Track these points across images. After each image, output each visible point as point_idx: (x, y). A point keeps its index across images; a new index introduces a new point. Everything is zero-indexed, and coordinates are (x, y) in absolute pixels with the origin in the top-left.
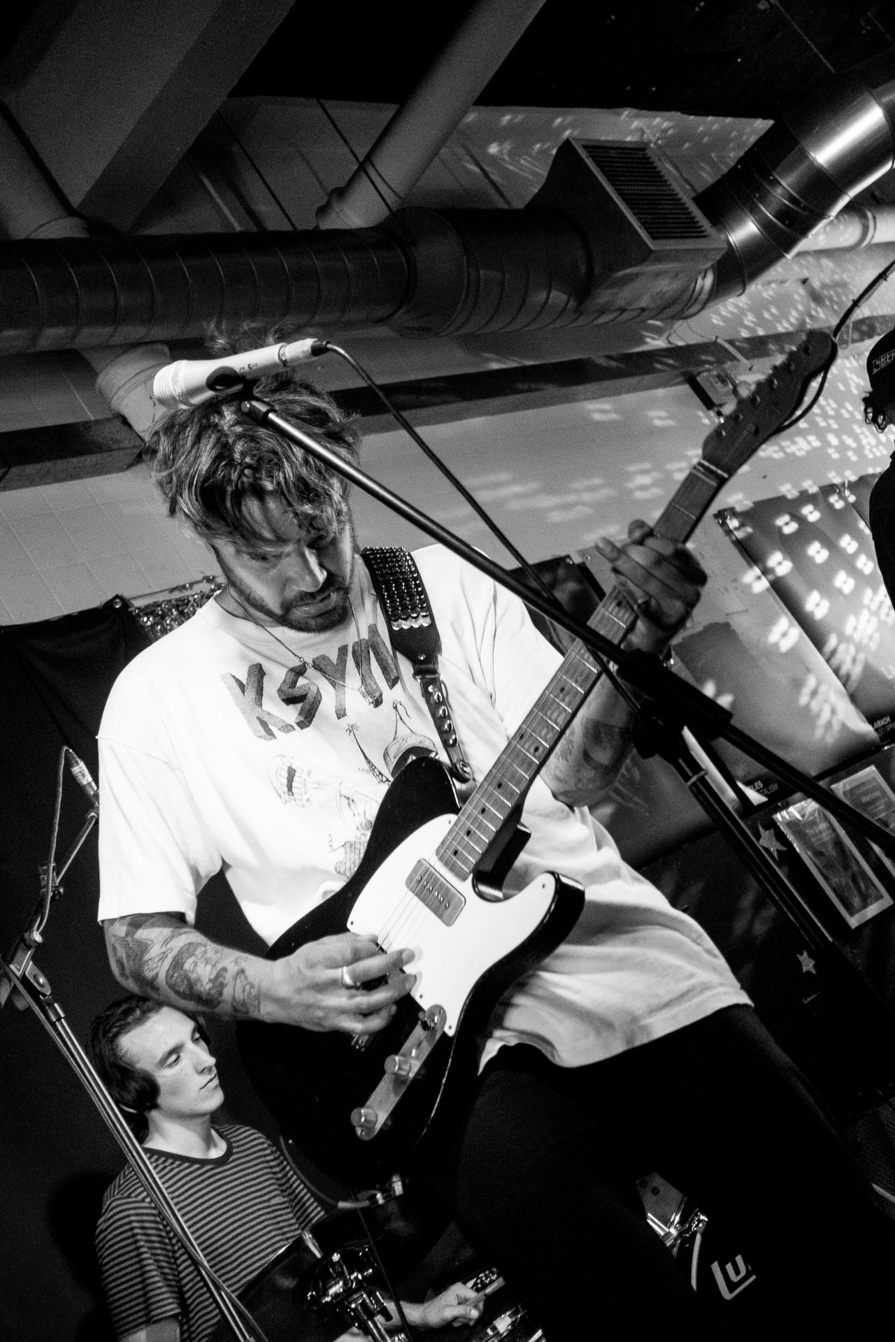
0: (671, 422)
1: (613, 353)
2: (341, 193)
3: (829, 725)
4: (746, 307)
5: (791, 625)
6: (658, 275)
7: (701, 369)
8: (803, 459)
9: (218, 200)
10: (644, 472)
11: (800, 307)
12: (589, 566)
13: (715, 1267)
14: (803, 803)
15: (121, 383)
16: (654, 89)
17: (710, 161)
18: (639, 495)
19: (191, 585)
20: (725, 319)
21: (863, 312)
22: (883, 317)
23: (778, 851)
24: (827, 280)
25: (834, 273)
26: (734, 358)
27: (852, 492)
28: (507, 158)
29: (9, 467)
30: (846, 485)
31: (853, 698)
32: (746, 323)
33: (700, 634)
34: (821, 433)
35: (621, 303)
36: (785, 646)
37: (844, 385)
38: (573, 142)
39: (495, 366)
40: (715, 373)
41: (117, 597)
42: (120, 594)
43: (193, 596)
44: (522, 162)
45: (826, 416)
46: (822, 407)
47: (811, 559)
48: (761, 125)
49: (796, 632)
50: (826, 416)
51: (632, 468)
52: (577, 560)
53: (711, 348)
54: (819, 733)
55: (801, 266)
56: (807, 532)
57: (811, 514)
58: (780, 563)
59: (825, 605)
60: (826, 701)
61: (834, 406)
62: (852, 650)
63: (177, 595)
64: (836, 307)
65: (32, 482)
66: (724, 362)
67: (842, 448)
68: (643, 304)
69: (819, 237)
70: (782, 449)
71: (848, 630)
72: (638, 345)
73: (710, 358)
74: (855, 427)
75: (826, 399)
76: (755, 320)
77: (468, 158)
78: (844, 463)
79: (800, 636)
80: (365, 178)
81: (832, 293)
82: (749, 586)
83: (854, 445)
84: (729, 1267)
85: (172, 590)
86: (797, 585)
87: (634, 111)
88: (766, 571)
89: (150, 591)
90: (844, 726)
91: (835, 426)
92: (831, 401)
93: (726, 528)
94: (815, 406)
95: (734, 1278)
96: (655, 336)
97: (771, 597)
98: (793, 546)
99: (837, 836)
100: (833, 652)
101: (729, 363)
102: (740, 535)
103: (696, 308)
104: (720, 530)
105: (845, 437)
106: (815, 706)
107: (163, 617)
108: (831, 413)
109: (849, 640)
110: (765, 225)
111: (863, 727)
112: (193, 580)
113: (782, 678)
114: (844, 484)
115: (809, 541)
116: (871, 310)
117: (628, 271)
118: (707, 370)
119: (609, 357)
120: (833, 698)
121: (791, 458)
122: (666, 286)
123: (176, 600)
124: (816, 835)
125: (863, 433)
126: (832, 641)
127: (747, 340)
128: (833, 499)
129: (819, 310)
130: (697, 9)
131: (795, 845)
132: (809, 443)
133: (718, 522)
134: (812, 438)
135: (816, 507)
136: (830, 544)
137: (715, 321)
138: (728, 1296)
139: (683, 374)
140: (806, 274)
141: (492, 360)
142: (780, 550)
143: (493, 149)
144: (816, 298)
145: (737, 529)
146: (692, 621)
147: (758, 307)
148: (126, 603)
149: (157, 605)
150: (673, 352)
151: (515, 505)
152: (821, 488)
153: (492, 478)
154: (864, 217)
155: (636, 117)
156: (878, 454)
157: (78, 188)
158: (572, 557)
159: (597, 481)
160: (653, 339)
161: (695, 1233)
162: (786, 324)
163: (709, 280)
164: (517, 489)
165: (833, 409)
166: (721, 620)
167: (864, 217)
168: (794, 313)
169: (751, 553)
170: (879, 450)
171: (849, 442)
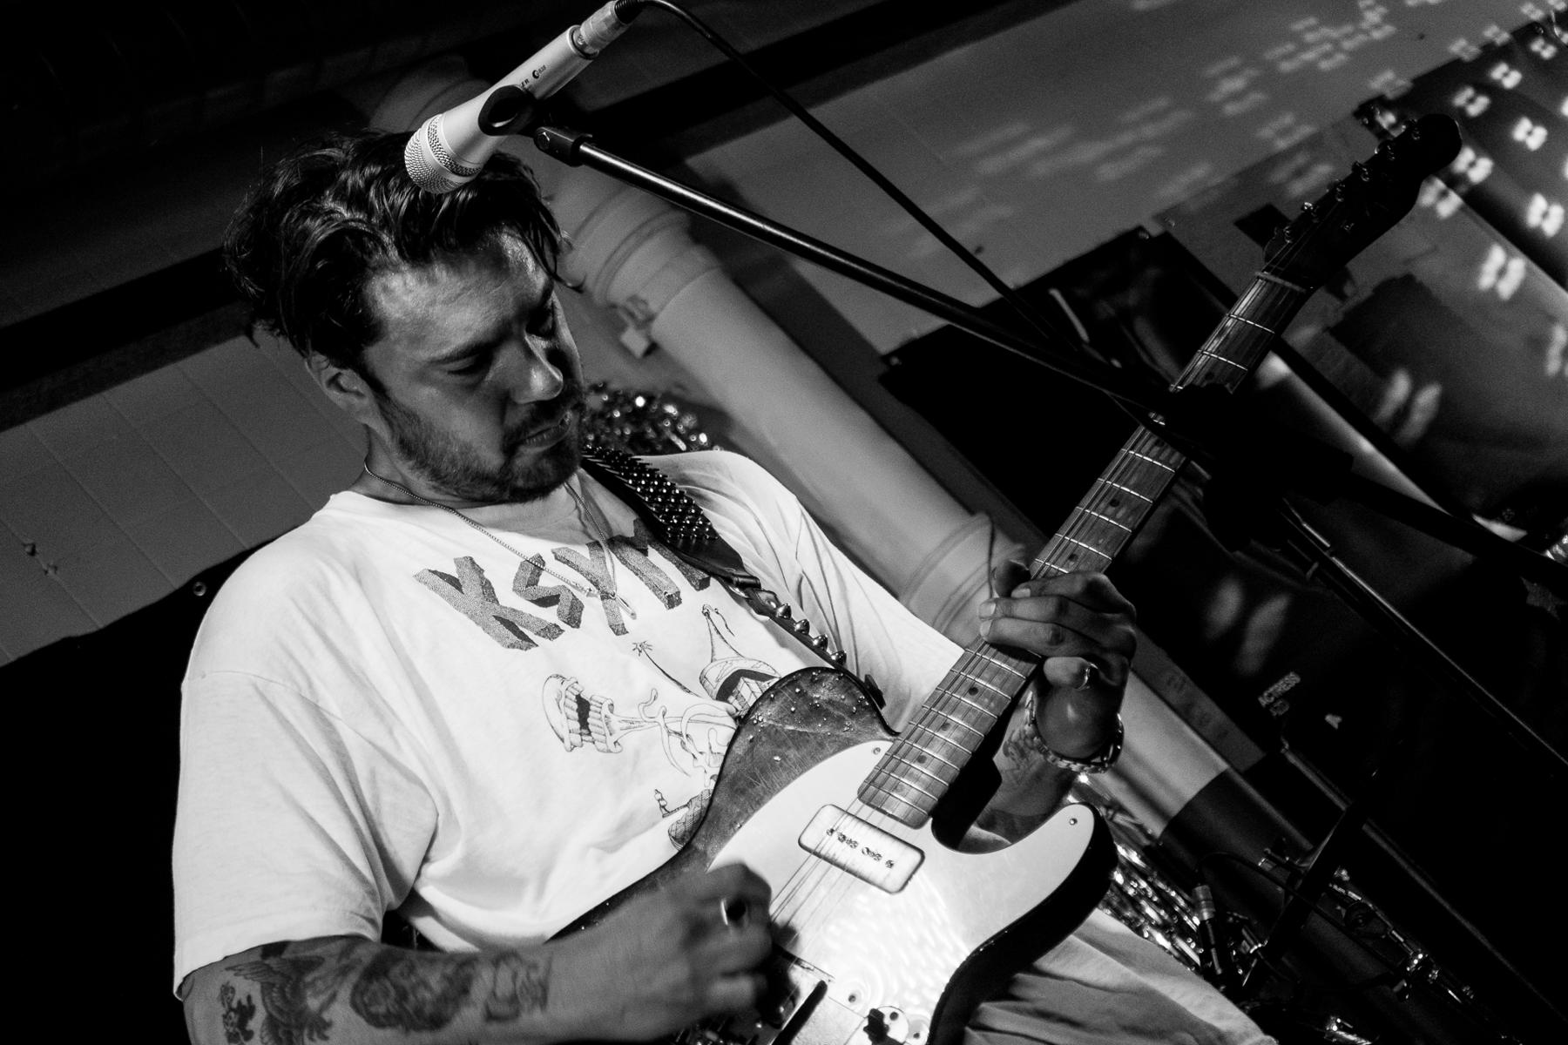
5: (1509, 255)
10: (1231, 73)
12: (1175, 235)
18: (1231, 109)
33: (1369, 300)
36: (1507, 288)
47: (1521, 146)
49: (1518, 266)
51: (1214, 70)
52: (1155, 230)
56: (1506, 106)
57: (1508, 77)
58: (1472, 165)
79: (1528, 269)
82: (1432, 210)
86: (1506, 191)
88: (1454, 182)
97: (1468, 220)
114: (1548, 19)
115: (1512, 120)
128: (1537, 46)
133: (1364, 124)
135: (1513, 65)
145: (1394, 126)
146: (1353, 283)
151: (1041, 169)
152: (1514, 33)
153: (997, 136)
158: (1145, 225)
159: (1162, 102)
164: (1039, 143)
166: (1397, 272)
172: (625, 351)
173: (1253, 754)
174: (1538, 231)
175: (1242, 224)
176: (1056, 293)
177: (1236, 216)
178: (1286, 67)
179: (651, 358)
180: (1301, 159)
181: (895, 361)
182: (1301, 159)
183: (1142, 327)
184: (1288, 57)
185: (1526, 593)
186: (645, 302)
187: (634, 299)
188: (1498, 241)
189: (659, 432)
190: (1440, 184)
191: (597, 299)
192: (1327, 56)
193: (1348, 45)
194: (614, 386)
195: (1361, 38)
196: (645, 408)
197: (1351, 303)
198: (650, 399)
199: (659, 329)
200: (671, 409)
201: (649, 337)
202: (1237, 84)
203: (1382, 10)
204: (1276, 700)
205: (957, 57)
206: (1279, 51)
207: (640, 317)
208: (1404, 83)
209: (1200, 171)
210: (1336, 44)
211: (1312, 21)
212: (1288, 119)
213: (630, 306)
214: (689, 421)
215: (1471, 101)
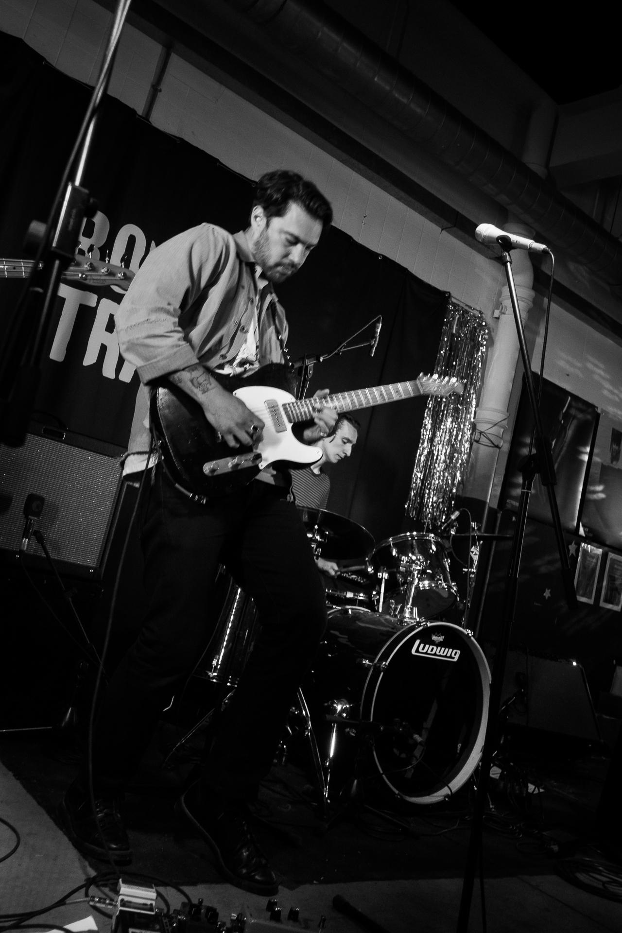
13: (418, 642)
19: (474, 309)
29: (455, 226)
33: (616, 469)
41: (449, 292)
52: (599, 411)
63: (467, 308)
65: (457, 237)
84: (422, 645)
85: (467, 305)
89: (460, 299)
95: (420, 650)
107: (457, 311)
112: (476, 308)
138: (413, 652)
148: (450, 296)
149: (458, 305)
151: (596, 377)
153: (597, 362)
161: (421, 626)
164: (602, 373)
173: (495, 506)
175: (613, 430)
176: (570, 398)
179: (495, 319)
183: (575, 422)
186: (507, 310)
187: (506, 307)
189: (480, 332)
191: (500, 299)
194: (483, 315)
196: (483, 326)
197: (612, 465)
199: (503, 317)
200: (486, 331)
205: (610, 342)
213: (504, 307)
214: (487, 337)
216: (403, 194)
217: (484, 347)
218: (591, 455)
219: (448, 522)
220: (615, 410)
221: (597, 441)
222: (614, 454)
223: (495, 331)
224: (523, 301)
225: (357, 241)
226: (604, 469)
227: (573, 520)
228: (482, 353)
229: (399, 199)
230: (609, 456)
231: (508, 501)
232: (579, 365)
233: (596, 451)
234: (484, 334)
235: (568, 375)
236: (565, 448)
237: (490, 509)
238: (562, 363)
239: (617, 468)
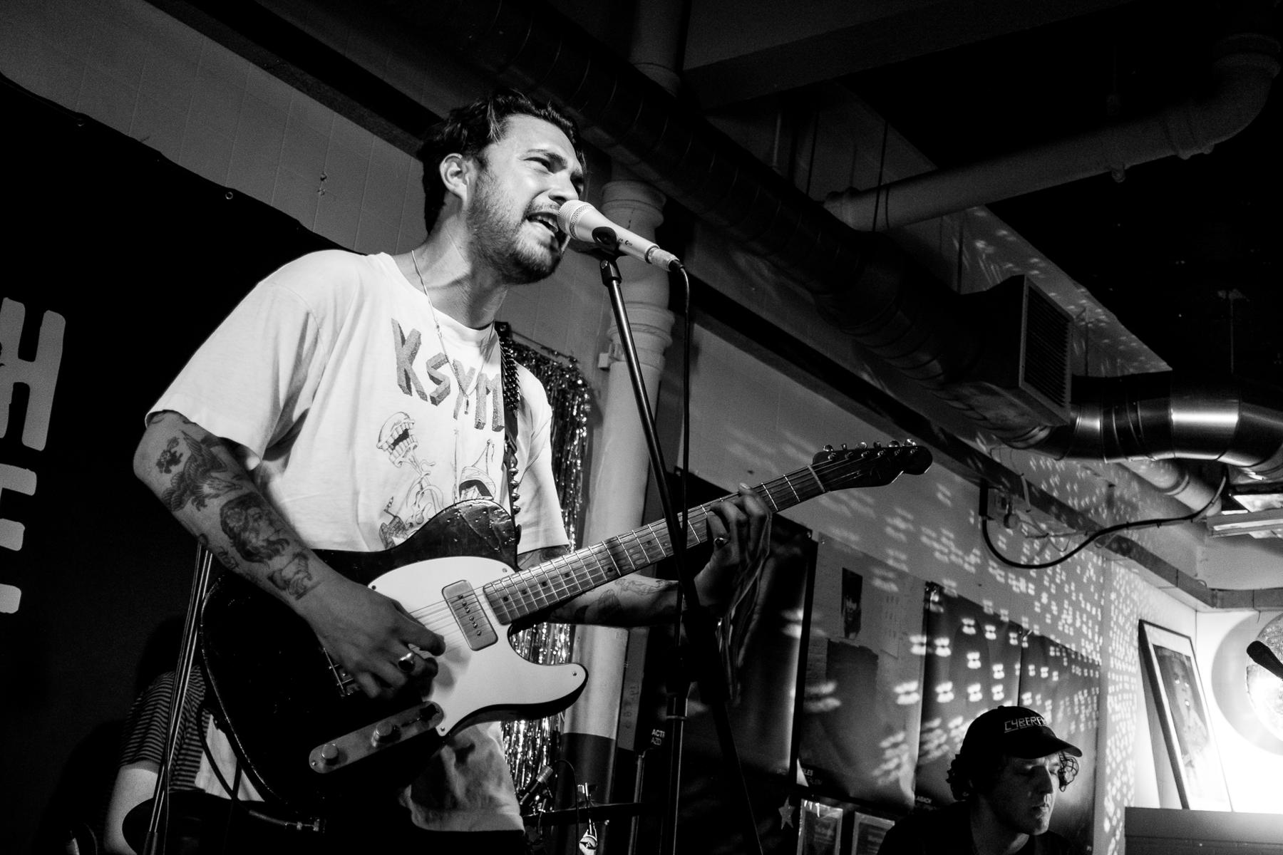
0: (948, 502)
1: (948, 430)
2: (854, 193)
3: (888, 773)
4: (1059, 470)
5: (917, 691)
6: (1012, 405)
7: (995, 486)
8: (1014, 593)
9: (777, 139)
10: (904, 519)
11: (1094, 499)
14: (829, 808)
15: (620, 198)
16: (1111, 289)
17: (1114, 365)
18: (889, 531)
19: (559, 354)
20: (1038, 466)
21: (1125, 533)
22: (1142, 548)
23: (786, 823)
24: (1126, 497)
25: (1135, 496)
26: (1023, 496)
27: (1028, 641)
28: (984, 256)
30: (1029, 633)
31: (918, 769)
32: (1051, 481)
33: (854, 647)
34: (1040, 588)
35: (973, 402)
36: (903, 700)
37: (1081, 571)
38: (1025, 279)
39: (866, 377)
40: (1003, 495)
41: (506, 324)
42: (509, 323)
43: (554, 362)
44: (992, 267)
45: (1052, 580)
46: (1054, 572)
47: (966, 661)
48: (1164, 366)
50: (1052, 580)
51: (899, 511)
52: (815, 538)
53: (1014, 478)
54: (877, 772)
55: (1117, 474)
56: (977, 642)
57: (991, 633)
58: (943, 647)
59: (950, 696)
60: (899, 756)
61: (1064, 578)
62: (943, 739)
63: (545, 353)
64: (1118, 518)
66: (1014, 493)
67: (1046, 608)
68: (988, 415)
69: (1140, 464)
70: (1006, 577)
71: (951, 725)
72: (964, 436)
73: (1008, 485)
74: (1066, 602)
75: (1061, 569)
76: (1058, 483)
77: (958, 235)
78: (1039, 618)
79: (918, 702)
80: (875, 195)
81: (1123, 507)
82: (911, 644)
83: (1055, 613)
85: (544, 348)
86: (943, 669)
87: (1088, 293)
88: (930, 644)
90: (897, 781)
91: (1053, 591)
92: (1064, 573)
93: (927, 596)
94: (1051, 568)
96: (985, 442)
98: (962, 644)
99: (833, 847)
100: (931, 730)
101: (1017, 496)
102: (933, 608)
103: (1020, 444)
104: (923, 594)
105: (1053, 603)
106: (889, 753)
108: (1058, 581)
109: (947, 731)
110: (1106, 428)
111: (909, 791)
112: (562, 352)
113: (884, 719)
114: (1028, 631)
115: (974, 649)
116: (1139, 539)
117: (994, 387)
118: (999, 489)
119: (942, 430)
120: (905, 758)
121: (1008, 587)
122: (1011, 416)
123: (541, 356)
124: (820, 834)
125: (1068, 610)
126: (936, 723)
127: (1041, 491)
128: (1013, 635)
129: (1105, 511)
130: (1177, 263)
131: (800, 829)
132: (1027, 587)
134: (1031, 586)
136: (986, 662)
137: (1031, 463)
139: (982, 480)
140: (1116, 481)
141: (864, 370)
142: (951, 641)
143: (980, 244)
144: (1110, 502)
145: (934, 603)
146: (856, 636)
147: (1067, 477)
149: (527, 349)
150: (987, 461)
152: (1010, 621)
154: (1182, 476)
155: (1087, 297)
156: (1066, 631)
157: (695, 60)
158: (814, 533)
160: (982, 443)
162: (1076, 502)
163: (1043, 434)
165: (1061, 580)
166: (875, 651)
167: (1182, 476)
168: (1087, 500)
169: (931, 626)
170: (1069, 630)
171: (1054, 608)
172: (597, 359)
173: (629, 745)
174: (937, 695)
175: (845, 571)
177: (846, 567)
178: (924, 539)
179: (602, 371)
180: (891, 575)
181: (678, 473)
182: (891, 575)
183: (771, 563)
184: (929, 537)
185: (782, 805)
188: (920, 681)
189: (573, 399)
190: (925, 640)
192: (942, 552)
193: (953, 558)
195: (960, 561)
196: (579, 386)
198: (584, 385)
201: (609, 365)
202: (902, 525)
203: (979, 561)
204: (659, 737)
206: (929, 532)
207: (615, 355)
208: (955, 593)
209: (854, 538)
210: (950, 552)
211: (952, 536)
212: (903, 557)
215: (969, 626)
216: (397, 131)
217: (585, 428)
218: (806, 624)
219: (531, 791)
220: (845, 534)
221: (815, 596)
222: (850, 619)
223: (602, 397)
224: (652, 333)
225: (310, 229)
226: (835, 650)
227: (783, 757)
228: (582, 439)
229: (392, 140)
230: (840, 623)
231: (654, 732)
232: (769, 450)
233: (815, 616)
234: (583, 402)
235: (751, 472)
236: (756, 617)
237: (620, 751)
238: (737, 450)
239: (857, 645)
